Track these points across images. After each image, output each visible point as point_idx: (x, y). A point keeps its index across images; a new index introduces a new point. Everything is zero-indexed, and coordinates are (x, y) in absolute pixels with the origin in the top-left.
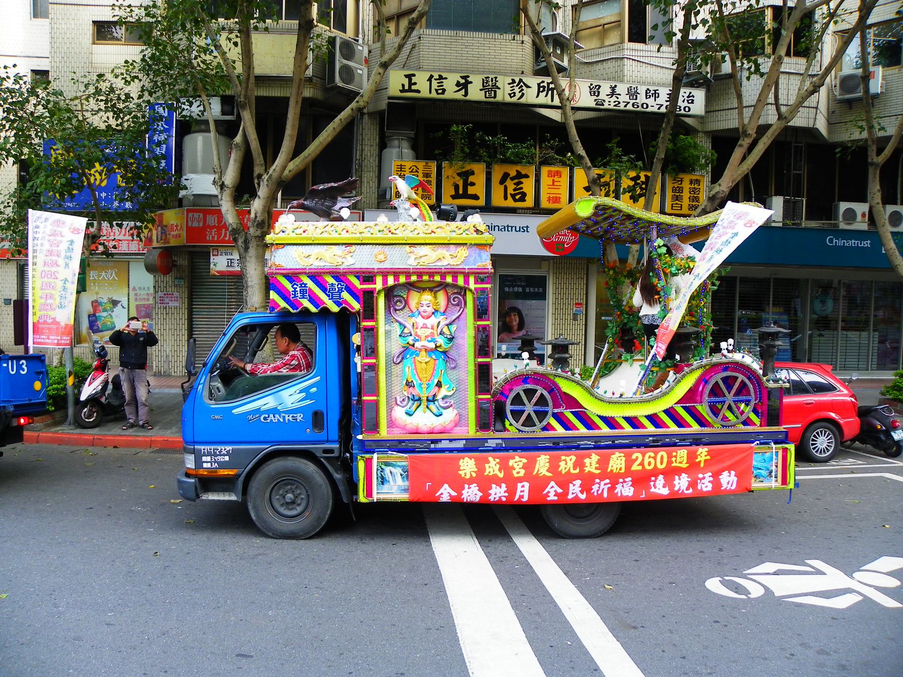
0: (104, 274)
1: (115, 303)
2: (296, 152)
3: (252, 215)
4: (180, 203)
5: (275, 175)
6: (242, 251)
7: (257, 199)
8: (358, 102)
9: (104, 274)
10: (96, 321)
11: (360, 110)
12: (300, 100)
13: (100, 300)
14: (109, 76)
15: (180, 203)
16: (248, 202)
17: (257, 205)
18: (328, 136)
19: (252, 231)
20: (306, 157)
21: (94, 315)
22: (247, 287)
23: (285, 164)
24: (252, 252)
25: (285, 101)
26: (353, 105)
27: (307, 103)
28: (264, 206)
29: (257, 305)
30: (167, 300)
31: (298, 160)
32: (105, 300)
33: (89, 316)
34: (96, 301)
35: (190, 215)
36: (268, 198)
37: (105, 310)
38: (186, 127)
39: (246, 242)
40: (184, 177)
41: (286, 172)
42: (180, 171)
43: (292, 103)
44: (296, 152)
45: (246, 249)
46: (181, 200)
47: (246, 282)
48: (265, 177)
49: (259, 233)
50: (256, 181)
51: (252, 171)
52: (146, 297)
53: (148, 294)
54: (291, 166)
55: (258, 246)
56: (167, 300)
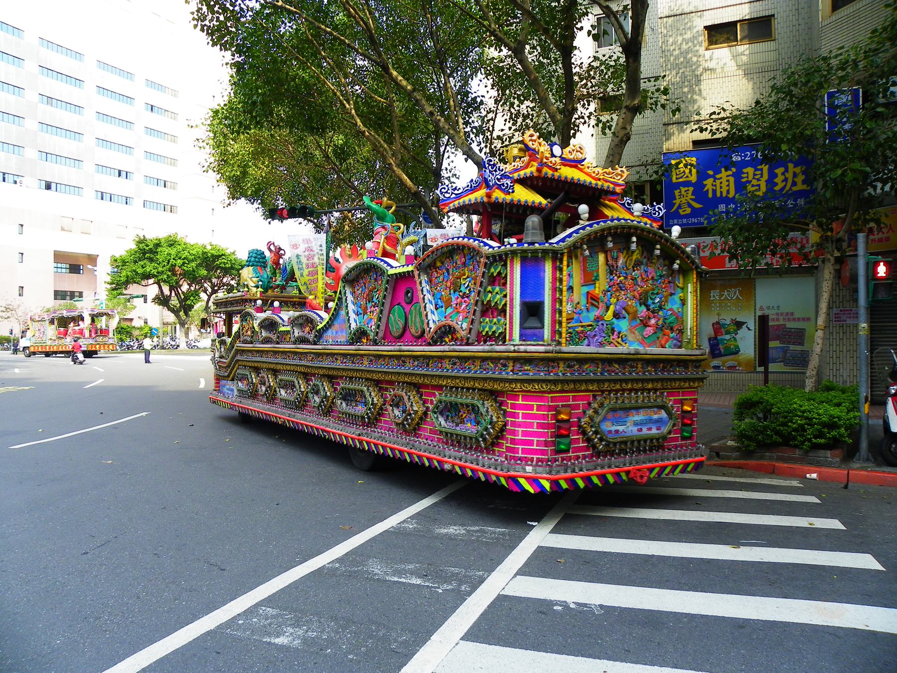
0: (726, 293)
1: (739, 325)
9: (726, 293)
10: (718, 344)
13: (722, 322)
21: (716, 338)
30: (843, 317)
32: (728, 322)
33: (710, 339)
34: (718, 323)
37: (728, 333)
52: (775, 317)
53: (777, 314)
56: (843, 317)
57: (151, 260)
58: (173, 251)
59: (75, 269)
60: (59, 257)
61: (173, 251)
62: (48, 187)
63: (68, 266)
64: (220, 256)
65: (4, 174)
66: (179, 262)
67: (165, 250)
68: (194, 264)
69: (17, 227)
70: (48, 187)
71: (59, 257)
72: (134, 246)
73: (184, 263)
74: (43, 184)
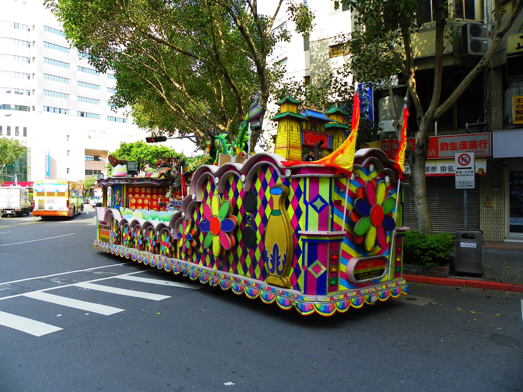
2: (441, 101)
3: (417, 142)
4: (378, 138)
5: (429, 117)
6: (411, 163)
7: (419, 132)
8: (481, 63)
11: (483, 68)
12: (441, 69)
14: (335, 74)
15: (378, 138)
16: (414, 135)
17: (419, 136)
18: (462, 89)
19: (416, 151)
20: (448, 103)
22: (415, 185)
23: (435, 109)
24: (417, 164)
25: (432, 71)
26: (479, 65)
27: (446, 70)
28: (423, 136)
29: (421, 195)
31: (443, 106)
35: (383, 144)
36: (425, 131)
38: (379, 95)
39: (413, 158)
40: (380, 123)
41: (436, 114)
42: (377, 120)
43: (436, 72)
44: (441, 101)
45: (414, 162)
46: (378, 136)
47: (414, 181)
48: (423, 118)
49: (421, 152)
50: (418, 121)
51: (416, 116)
54: (439, 110)
55: (420, 160)
57: (128, 155)
58: (139, 150)
59: (96, 158)
60: (88, 152)
61: (139, 150)
62: (82, 115)
63: (93, 157)
64: (165, 152)
65: (60, 109)
66: (142, 156)
67: (134, 150)
68: (150, 157)
69: (66, 137)
70: (82, 115)
71: (88, 152)
72: (119, 148)
73: (145, 156)
74: (80, 113)
